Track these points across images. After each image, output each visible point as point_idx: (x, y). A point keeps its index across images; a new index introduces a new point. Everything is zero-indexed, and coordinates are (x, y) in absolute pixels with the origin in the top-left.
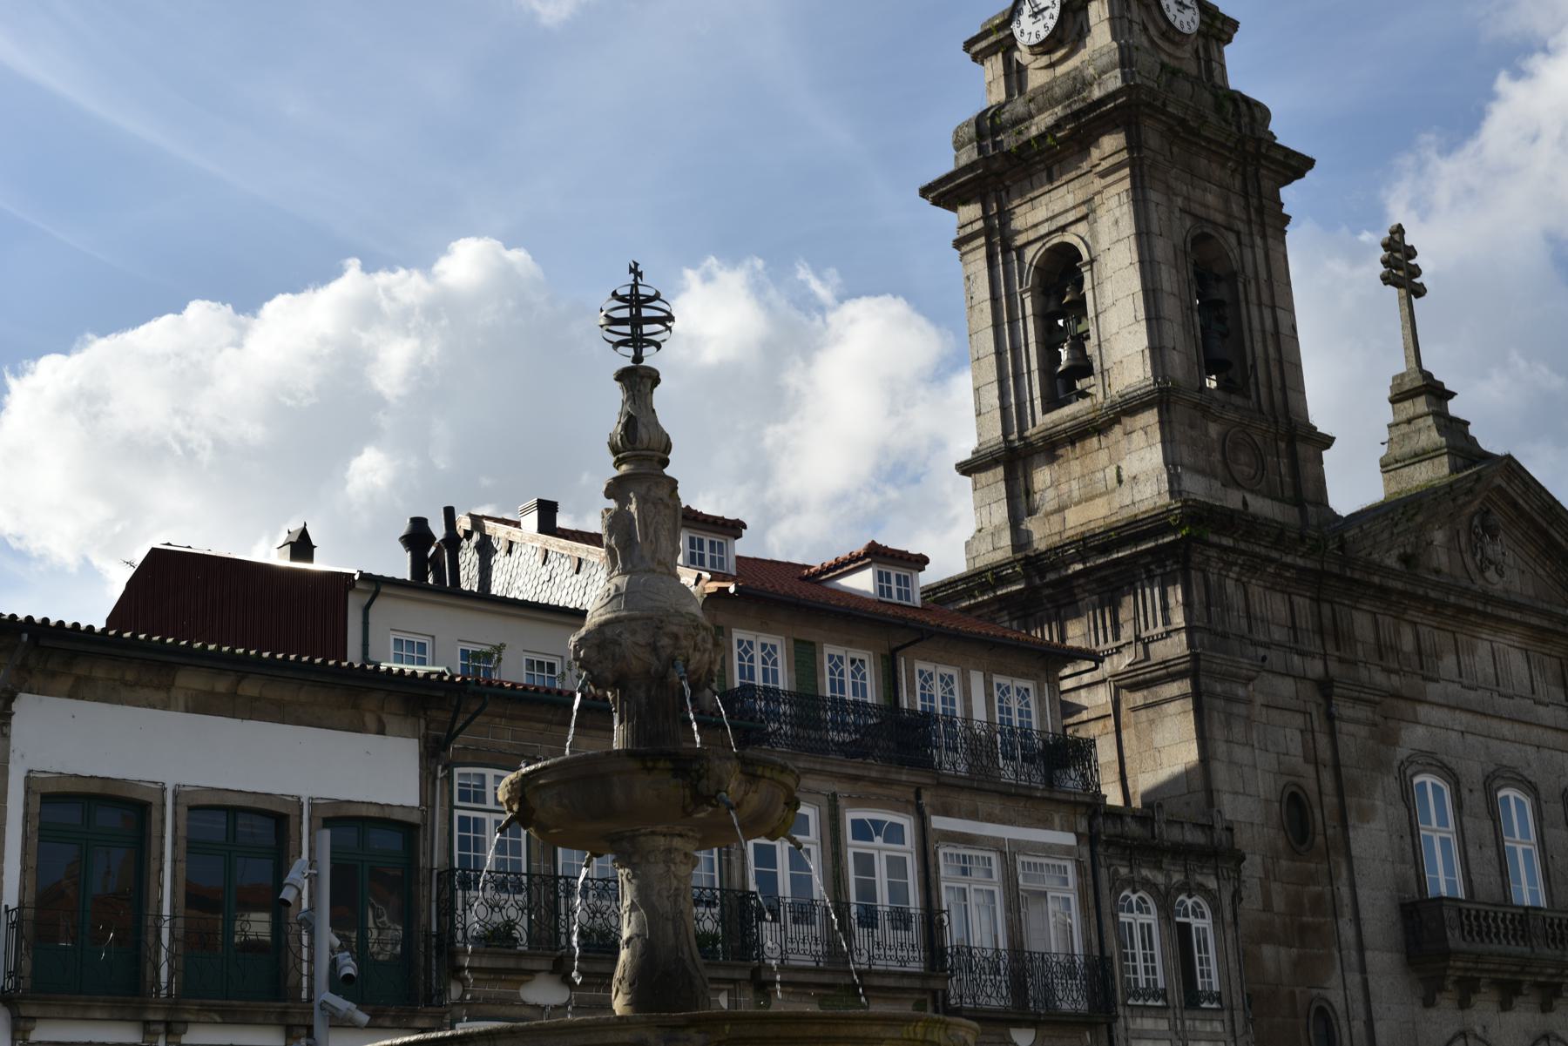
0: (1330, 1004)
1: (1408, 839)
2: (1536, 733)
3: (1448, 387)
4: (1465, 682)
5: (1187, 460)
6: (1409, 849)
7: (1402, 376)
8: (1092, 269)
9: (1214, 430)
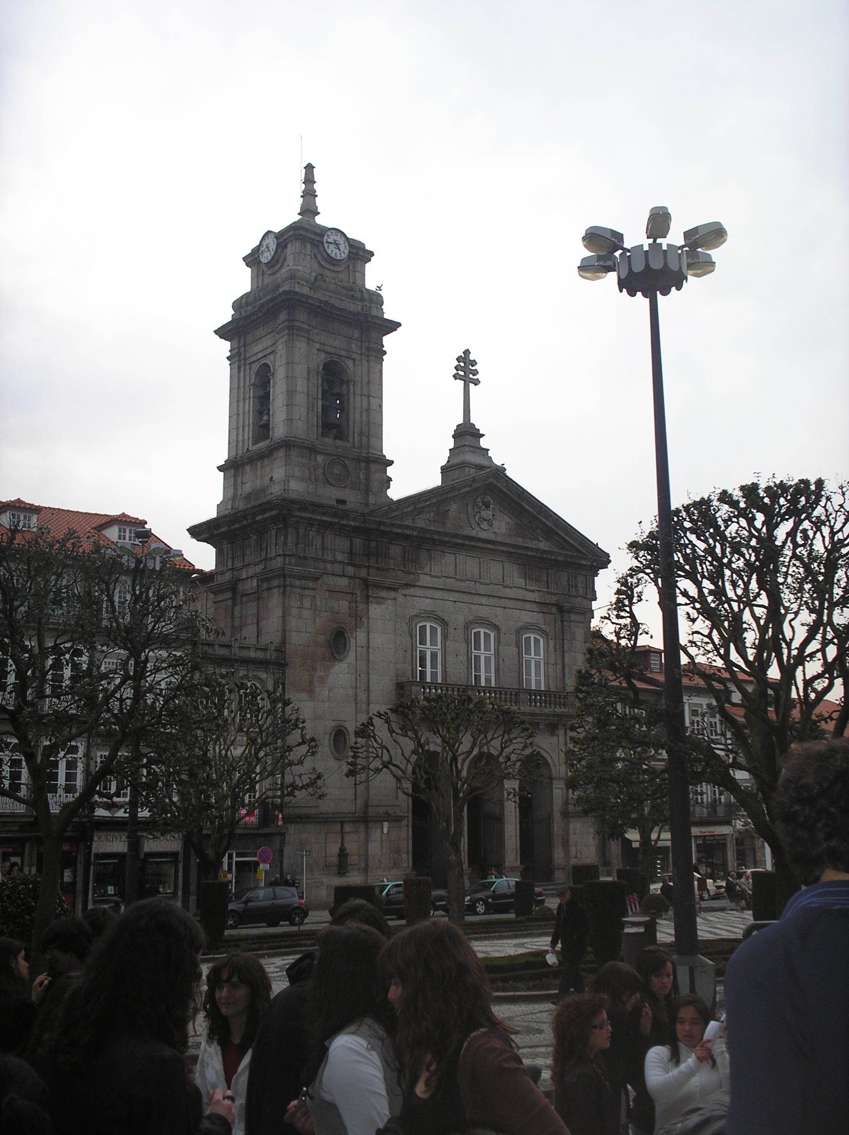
0: (345, 728)
1: (409, 652)
2: (502, 603)
4: (458, 577)
5: (297, 473)
6: (409, 656)
9: (320, 459)
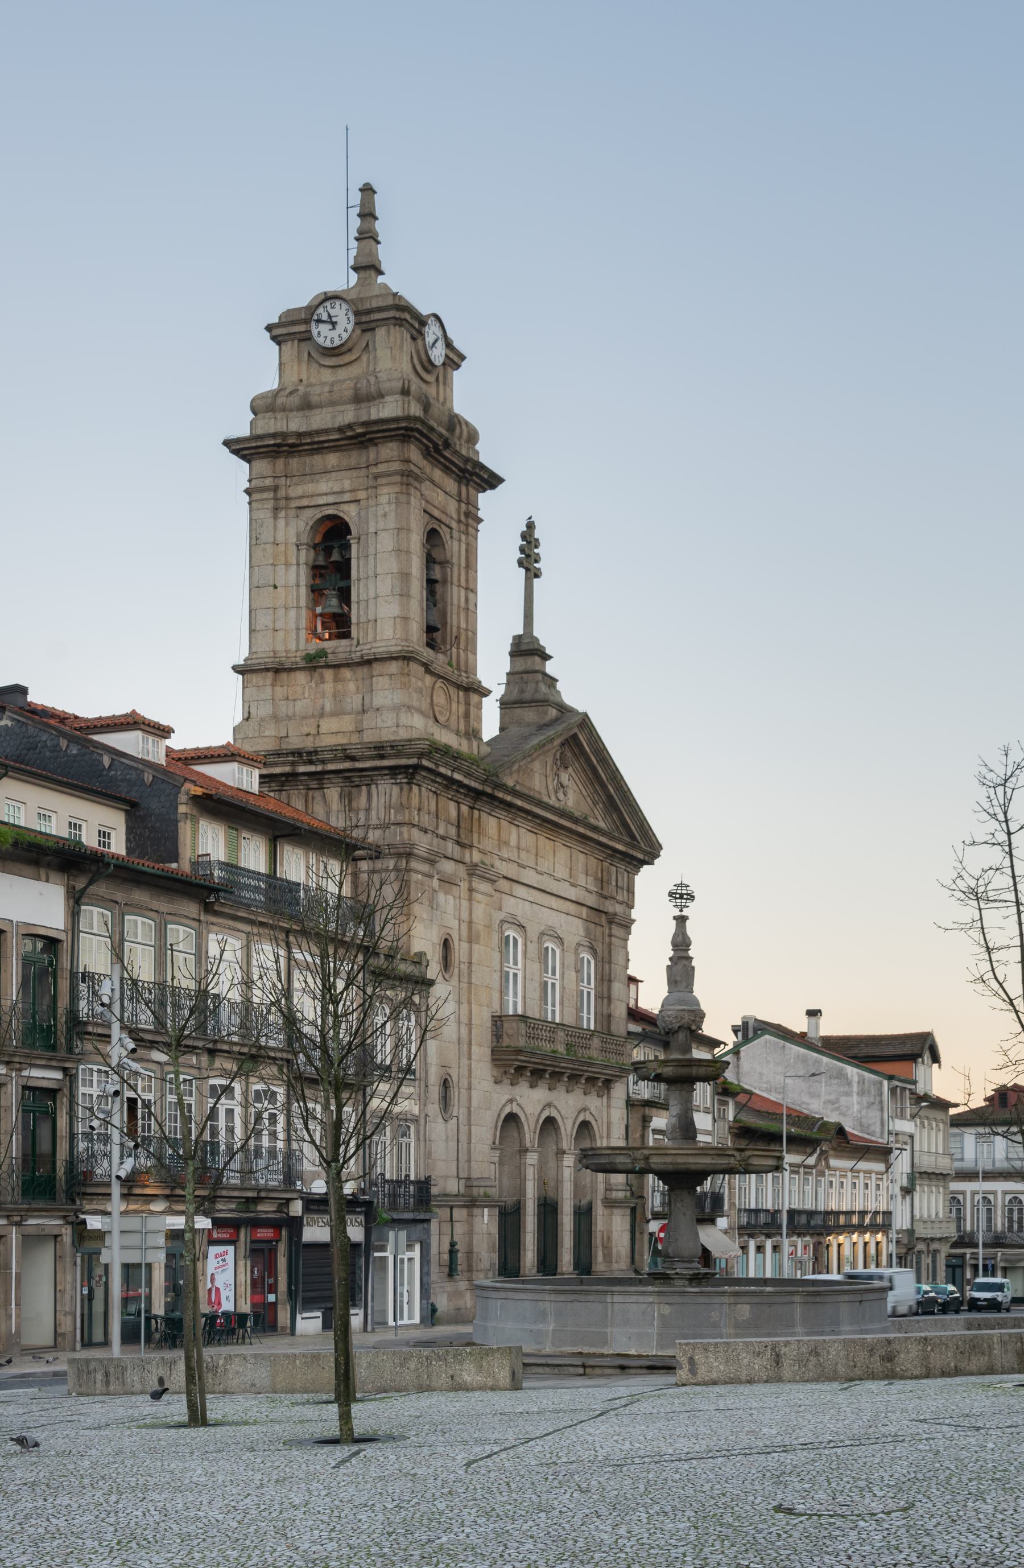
3: (548, 652)
7: (520, 636)
8: (358, 543)
